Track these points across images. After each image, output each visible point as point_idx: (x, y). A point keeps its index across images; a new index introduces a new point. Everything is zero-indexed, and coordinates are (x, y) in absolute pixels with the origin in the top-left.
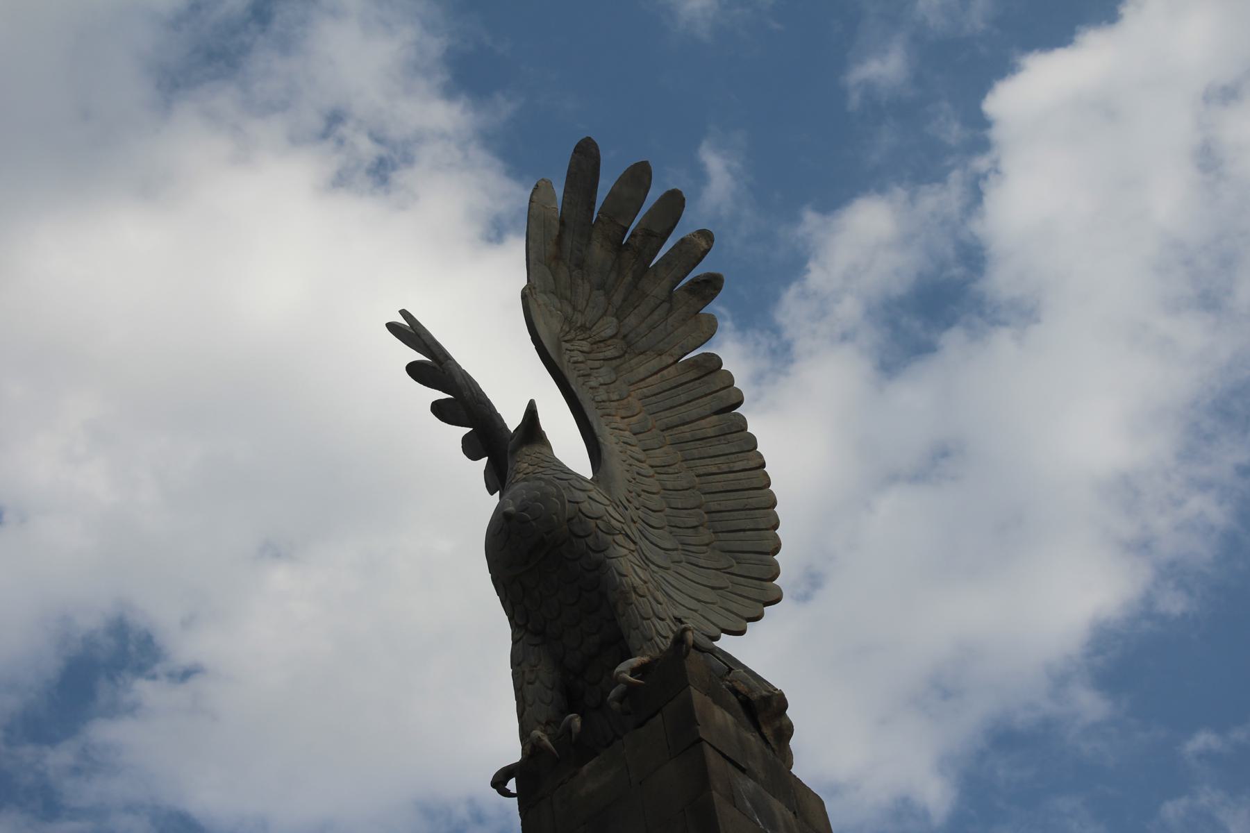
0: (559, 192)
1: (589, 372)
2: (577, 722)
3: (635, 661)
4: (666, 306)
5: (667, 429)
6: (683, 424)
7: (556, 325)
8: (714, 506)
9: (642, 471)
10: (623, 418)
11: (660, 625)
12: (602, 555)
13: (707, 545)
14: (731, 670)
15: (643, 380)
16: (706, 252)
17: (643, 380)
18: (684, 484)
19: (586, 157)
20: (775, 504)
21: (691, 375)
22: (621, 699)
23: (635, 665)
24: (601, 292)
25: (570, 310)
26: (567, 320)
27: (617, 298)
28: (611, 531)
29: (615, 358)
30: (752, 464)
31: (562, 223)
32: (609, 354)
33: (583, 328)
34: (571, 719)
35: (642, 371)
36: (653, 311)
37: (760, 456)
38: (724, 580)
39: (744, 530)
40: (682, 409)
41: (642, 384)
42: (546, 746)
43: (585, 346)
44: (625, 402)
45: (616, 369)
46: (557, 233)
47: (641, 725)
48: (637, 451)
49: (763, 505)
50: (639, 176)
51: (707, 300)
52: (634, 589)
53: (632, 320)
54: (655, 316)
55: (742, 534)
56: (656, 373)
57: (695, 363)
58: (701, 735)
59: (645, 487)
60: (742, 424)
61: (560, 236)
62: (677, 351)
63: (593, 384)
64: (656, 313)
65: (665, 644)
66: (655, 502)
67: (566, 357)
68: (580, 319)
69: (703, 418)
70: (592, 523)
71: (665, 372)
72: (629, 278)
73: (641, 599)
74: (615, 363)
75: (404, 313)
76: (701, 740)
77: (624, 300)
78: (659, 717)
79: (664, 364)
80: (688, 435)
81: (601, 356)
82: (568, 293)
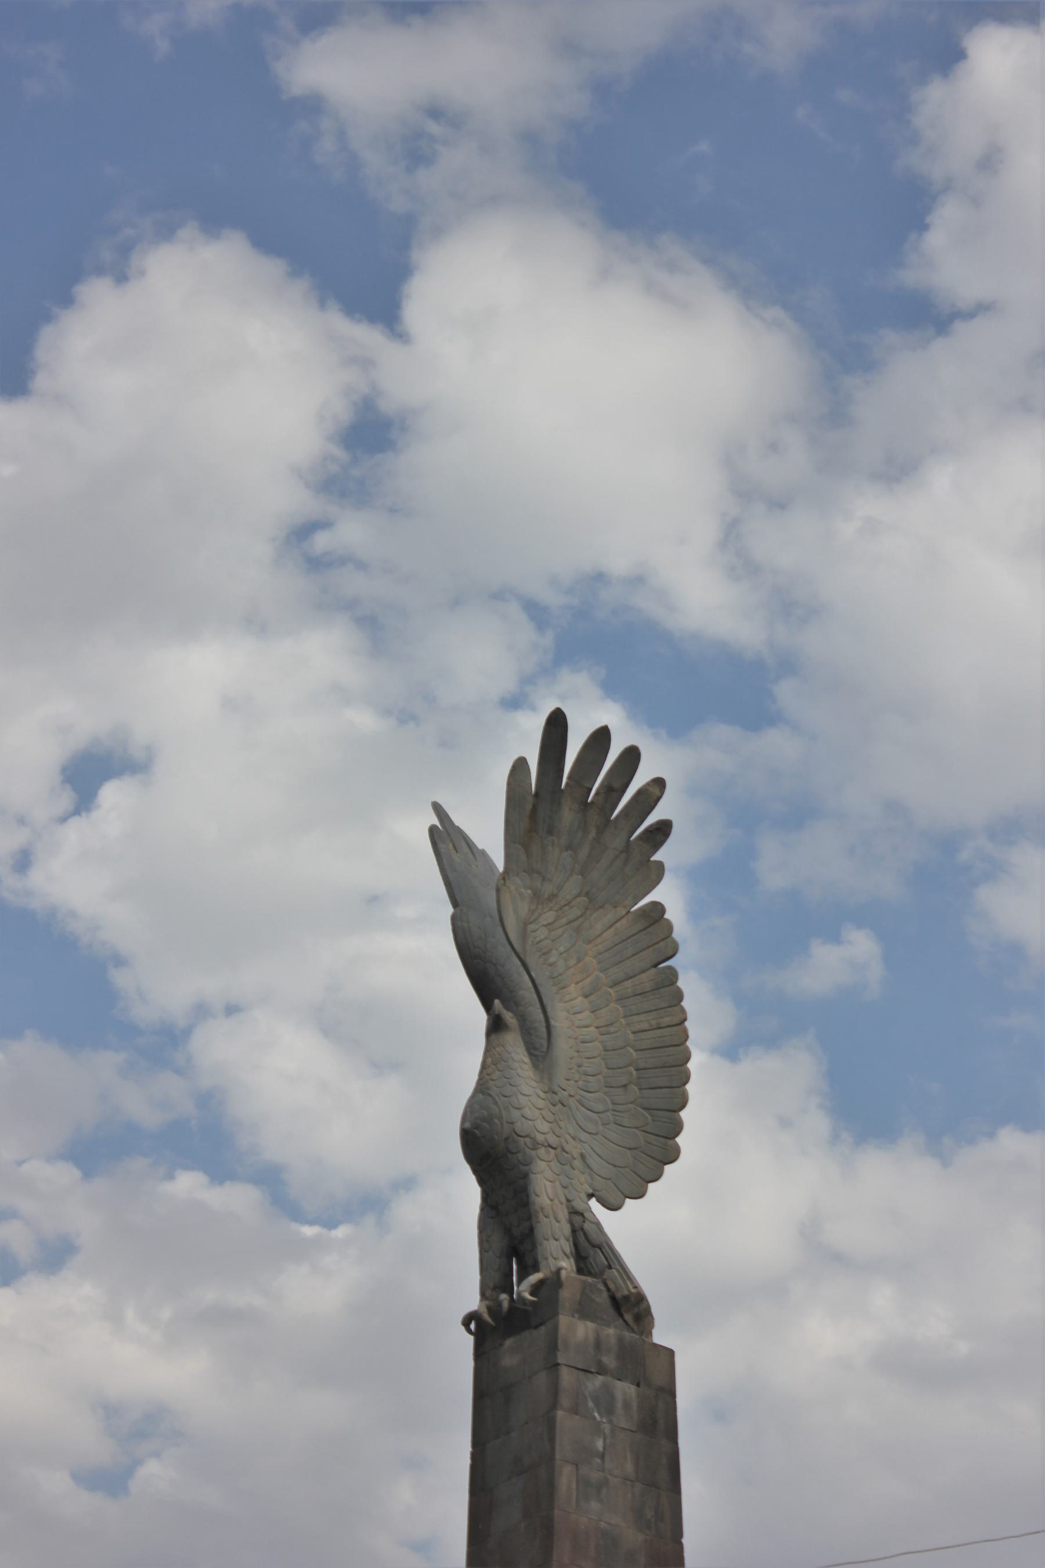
6: (627, 979)
7: (524, 908)
10: (577, 983)
12: (526, 1168)
13: (632, 1103)
14: (610, 1267)
15: (600, 935)
17: (600, 935)
19: (556, 726)
20: (688, 1059)
26: (536, 895)
27: (583, 853)
28: (536, 1145)
29: (577, 919)
30: (676, 1021)
31: (537, 795)
32: (571, 916)
33: (553, 897)
37: (683, 1011)
39: (661, 1088)
41: (599, 940)
43: (549, 916)
44: (580, 965)
46: (529, 807)
48: (585, 1016)
50: (601, 738)
51: (657, 846)
52: (542, 1209)
55: (659, 1090)
56: (611, 927)
57: (644, 912)
58: (559, 1361)
60: (672, 976)
61: (534, 808)
63: (552, 960)
68: (548, 889)
69: (643, 972)
71: (618, 925)
72: (593, 834)
74: (577, 923)
76: (558, 1364)
81: (564, 921)
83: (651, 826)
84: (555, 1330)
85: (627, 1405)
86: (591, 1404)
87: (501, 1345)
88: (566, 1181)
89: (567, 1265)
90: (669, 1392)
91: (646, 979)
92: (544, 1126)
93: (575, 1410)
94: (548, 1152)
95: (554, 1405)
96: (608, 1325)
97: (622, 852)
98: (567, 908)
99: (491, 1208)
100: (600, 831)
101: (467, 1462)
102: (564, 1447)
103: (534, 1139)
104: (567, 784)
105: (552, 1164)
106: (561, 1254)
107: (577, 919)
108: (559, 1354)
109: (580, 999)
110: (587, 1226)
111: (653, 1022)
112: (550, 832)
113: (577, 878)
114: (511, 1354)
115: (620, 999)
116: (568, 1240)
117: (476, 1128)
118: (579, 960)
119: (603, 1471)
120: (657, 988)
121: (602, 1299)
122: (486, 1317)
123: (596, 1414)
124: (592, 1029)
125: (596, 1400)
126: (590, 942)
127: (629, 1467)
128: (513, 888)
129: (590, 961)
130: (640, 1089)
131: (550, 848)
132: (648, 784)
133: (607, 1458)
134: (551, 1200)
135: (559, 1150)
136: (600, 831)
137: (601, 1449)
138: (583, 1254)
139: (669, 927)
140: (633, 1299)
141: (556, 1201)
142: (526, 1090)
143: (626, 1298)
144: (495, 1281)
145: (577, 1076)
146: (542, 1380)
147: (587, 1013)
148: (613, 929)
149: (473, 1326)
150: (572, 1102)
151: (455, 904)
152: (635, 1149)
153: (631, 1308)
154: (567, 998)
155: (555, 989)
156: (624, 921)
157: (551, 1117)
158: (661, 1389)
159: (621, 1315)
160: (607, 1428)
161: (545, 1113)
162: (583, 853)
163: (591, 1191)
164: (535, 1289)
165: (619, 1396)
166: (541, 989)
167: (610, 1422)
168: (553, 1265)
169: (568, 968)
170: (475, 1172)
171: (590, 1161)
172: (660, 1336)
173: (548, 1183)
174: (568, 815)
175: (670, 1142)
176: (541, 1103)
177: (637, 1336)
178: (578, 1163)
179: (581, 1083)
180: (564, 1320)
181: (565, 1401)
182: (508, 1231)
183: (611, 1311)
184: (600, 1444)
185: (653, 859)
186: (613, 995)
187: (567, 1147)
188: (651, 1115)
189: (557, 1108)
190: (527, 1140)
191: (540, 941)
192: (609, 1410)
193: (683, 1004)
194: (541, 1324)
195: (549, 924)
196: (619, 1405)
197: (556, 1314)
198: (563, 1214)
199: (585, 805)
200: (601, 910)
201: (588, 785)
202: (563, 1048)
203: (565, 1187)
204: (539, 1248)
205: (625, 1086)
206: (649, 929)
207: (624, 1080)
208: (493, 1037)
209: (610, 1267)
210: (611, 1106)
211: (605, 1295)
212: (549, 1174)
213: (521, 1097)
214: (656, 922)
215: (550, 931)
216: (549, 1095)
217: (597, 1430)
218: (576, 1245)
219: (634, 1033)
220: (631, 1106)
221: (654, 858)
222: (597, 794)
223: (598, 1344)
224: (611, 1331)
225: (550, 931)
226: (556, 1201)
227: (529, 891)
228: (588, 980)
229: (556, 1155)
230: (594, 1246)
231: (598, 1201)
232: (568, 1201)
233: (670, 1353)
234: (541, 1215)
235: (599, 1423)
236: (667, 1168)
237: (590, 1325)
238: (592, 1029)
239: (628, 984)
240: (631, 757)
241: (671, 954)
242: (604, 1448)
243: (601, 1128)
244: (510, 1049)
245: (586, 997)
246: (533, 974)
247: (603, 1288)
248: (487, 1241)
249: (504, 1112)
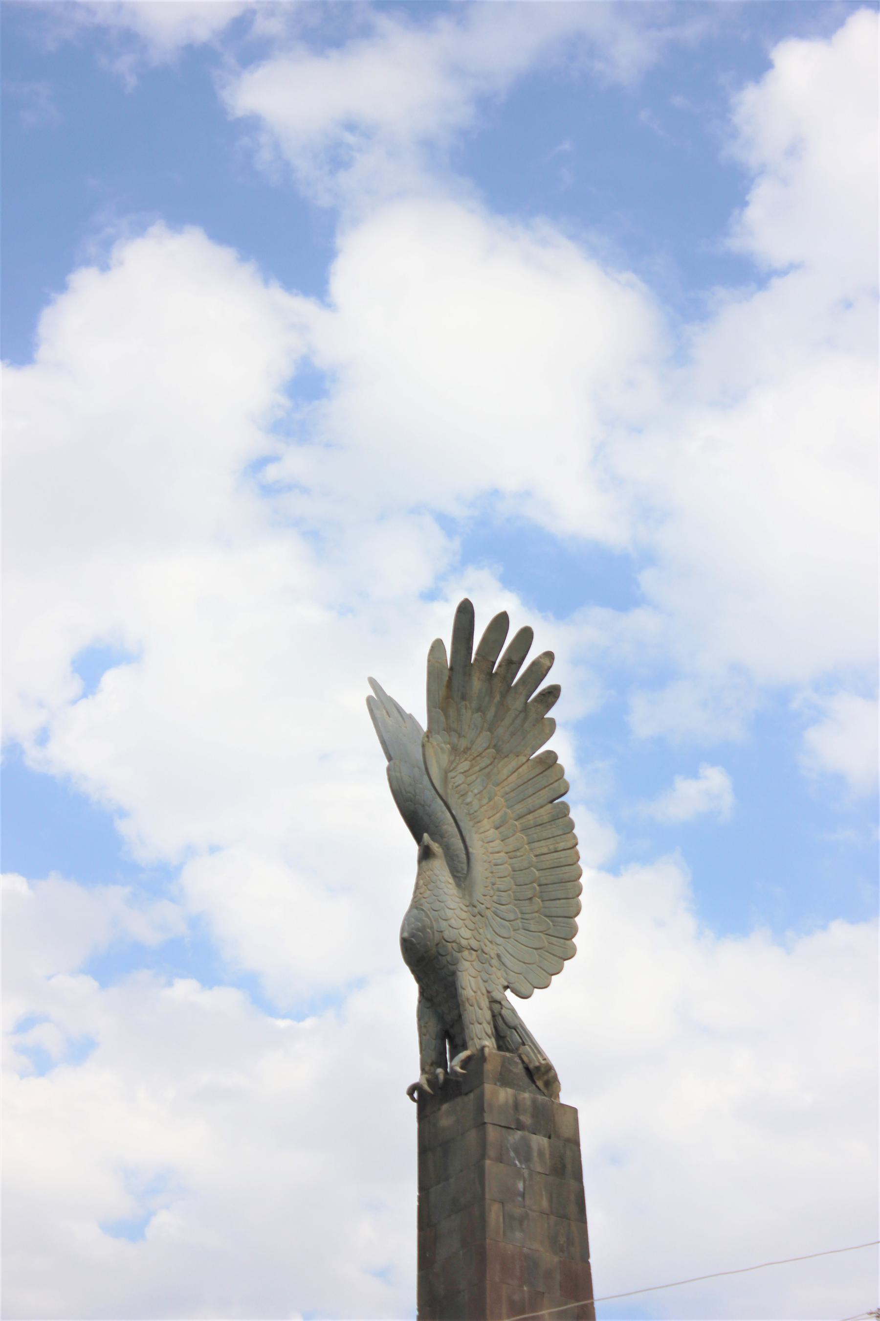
3: (463, 1055)
4: (522, 715)
7: (445, 759)
8: (544, 881)
10: (489, 818)
12: (454, 967)
14: (524, 1044)
16: (549, 668)
18: (525, 864)
19: (466, 612)
20: (580, 875)
21: (538, 771)
25: (455, 739)
26: (454, 749)
27: (490, 715)
28: (461, 949)
29: (487, 766)
30: (569, 845)
31: (451, 669)
32: (483, 765)
33: (468, 749)
35: (505, 772)
37: (575, 837)
40: (530, 800)
41: (505, 783)
43: (465, 765)
44: (491, 803)
46: (446, 678)
48: (497, 845)
49: (572, 879)
50: (501, 622)
51: (549, 706)
52: (468, 999)
53: (500, 731)
55: (558, 901)
58: (486, 1121)
59: (500, 875)
60: (565, 810)
61: (450, 678)
63: (468, 800)
68: (463, 743)
69: (542, 807)
71: (520, 770)
72: (497, 698)
74: (487, 770)
76: (485, 1123)
77: (495, 716)
79: (520, 763)
80: (531, 822)
81: (477, 768)
83: (544, 690)
84: (482, 1094)
85: (541, 1153)
86: (512, 1154)
87: (439, 1109)
88: (486, 976)
89: (489, 1044)
90: (575, 1142)
91: (544, 813)
92: (466, 933)
93: (500, 1159)
94: (471, 954)
95: (483, 1156)
96: (525, 1092)
97: (521, 712)
99: (427, 999)
100: (504, 696)
101: (416, 1204)
102: (492, 1189)
103: (459, 944)
104: (476, 659)
105: (474, 963)
106: (484, 1034)
107: (487, 766)
108: (485, 1115)
109: (492, 831)
110: (504, 1012)
111: (551, 847)
112: (464, 697)
114: (447, 1117)
115: (524, 829)
116: (489, 1024)
117: (413, 937)
118: (490, 800)
119: (524, 1207)
120: (554, 819)
121: (519, 1069)
122: (426, 1087)
123: (517, 1162)
124: (502, 854)
125: (516, 1151)
126: (498, 785)
127: (545, 1203)
128: (435, 743)
129: (499, 800)
130: (543, 901)
132: (540, 657)
133: (527, 1196)
134: (475, 992)
135: (479, 952)
136: (504, 696)
137: (522, 1190)
138: (502, 1035)
139: (561, 770)
140: (543, 1069)
141: (479, 993)
142: (452, 905)
143: (538, 1068)
144: (433, 1059)
145: (492, 892)
146: (472, 1136)
147: (498, 842)
148: (516, 774)
149: (416, 1095)
150: (489, 913)
151: (390, 758)
153: (541, 1076)
154: (482, 830)
155: (471, 823)
156: (525, 767)
157: (472, 926)
158: (568, 1140)
159: (534, 1082)
160: (526, 1172)
161: (467, 922)
162: (490, 715)
163: (506, 984)
164: (465, 1064)
165: (535, 1147)
166: (461, 824)
167: (528, 1168)
168: (478, 1044)
169: (481, 807)
170: (413, 971)
171: (504, 960)
172: (566, 1098)
173: (471, 979)
174: (477, 684)
175: (568, 942)
176: (464, 915)
177: (547, 1098)
178: (495, 962)
179: (495, 898)
180: (488, 1088)
181: (492, 1152)
182: (440, 1018)
183: (526, 1079)
184: (520, 1186)
185: (546, 716)
186: (519, 826)
187: (486, 949)
188: (552, 921)
189: (476, 918)
190: (454, 944)
191: (459, 785)
192: (527, 1159)
193: (575, 831)
194: (471, 1091)
195: (465, 772)
196: (535, 1154)
197: (483, 1083)
198: (485, 1003)
199: (490, 675)
200: (506, 759)
201: (492, 659)
202: (480, 870)
203: (484, 981)
204: (467, 1031)
205: (530, 899)
207: (529, 894)
208: (424, 863)
209: (524, 1044)
210: (520, 916)
211: (521, 1066)
212: (472, 972)
213: (447, 910)
214: (550, 767)
215: (466, 777)
216: (470, 908)
217: (518, 1174)
218: (496, 1027)
219: (536, 856)
220: (536, 914)
221: (547, 716)
222: (500, 666)
223: (516, 1106)
224: (526, 1095)
225: (466, 777)
226: (479, 993)
227: (448, 746)
228: (498, 815)
229: (477, 956)
230: (510, 1027)
231: (512, 991)
232: (488, 992)
233: (575, 1111)
234: (467, 1005)
235: (519, 1170)
236: (566, 963)
237: (510, 1091)
238: (502, 854)
239: (530, 817)
240: (526, 636)
241: (563, 792)
242: (524, 1189)
243: (512, 933)
244: (438, 872)
245: (497, 828)
246: (454, 812)
247: (519, 1061)
248: (425, 1027)
249: (434, 923)
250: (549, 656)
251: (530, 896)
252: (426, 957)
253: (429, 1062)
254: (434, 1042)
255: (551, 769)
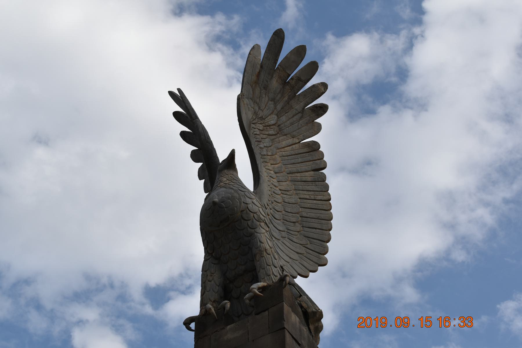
0: (263, 51)
1: (261, 140)
2: (228, 305)
3: (260, 284)
4: (300, 115)
5: (290, 173)
6: (298, 173)
7: (250, 115)
8: (304, 214)
9: (276, 192)
10: (271, 164)
11: (274, 270)
12: (253, 230)
13: (298, 232)
15: (284, 148)
17: (284, 148)
18: (293, 201)
19: (278, 37)
20: (331, 219)
22: (250, 299)
23: (260, 286)
24: (273, 102)
25: (257, 108)
26: (255, 113)
27: (279, 107)
28: (259, 220)
30: (325, 198)
31: (261, 67)
33: (262, 118)
34: (226, 303)
35: (284, 143)
36: (293, 117)
37: (329, 195)
38: (303, 250)
39: (316, 228)
40: (298, 165)
41: (283, 150)
42: (213, 313)
44: (273, 157)
45: (272, 140)
46: (258, 71)
47: (257, 314)
49: (327, 218)
50: (300, 51)
52: (266, 250)
53: (284, 118)
54: (294, 119)
55: (314, 230)
56: (290, 146)
59: (276, 199)
60: (323, 178)
61: (259, 73)
62: (301, 137)
63: (262, 146)
64: (295, 117)
65: (276, 279)
66: (279, 207)
67: (252, 131)
68: (261, 114)
70: (252, 215)
71: (294, 146)
72: (286, 98)
73: (268, 256)
74: (273, 137)
75: (179, 90)
77: (282, 108)
78: (267, 312)
79: (294, 142)
81: (267, 133)
82: (258, 101)
98: (268, 128)
100: (290, 99)
113: (274, 117)
124: (277, 189)
128: (245, 102)
131: (264, 96)
132: (319, 84)
134: (271, 248)
136: (290, 99)
139: (322, 154)
152: (300, 254)
156: (296, 145)
175: (322, 256)
190: (255, 215)
194: (267, 309)
206: (311, 153)
214: (314, 151)
221: (318, 121)
240: (313, 68)
250: (325, 86)
251: (295, 221)
252: (225, 226)
253: (213, 300)
254: (217, 287)
255: (315, 152)
